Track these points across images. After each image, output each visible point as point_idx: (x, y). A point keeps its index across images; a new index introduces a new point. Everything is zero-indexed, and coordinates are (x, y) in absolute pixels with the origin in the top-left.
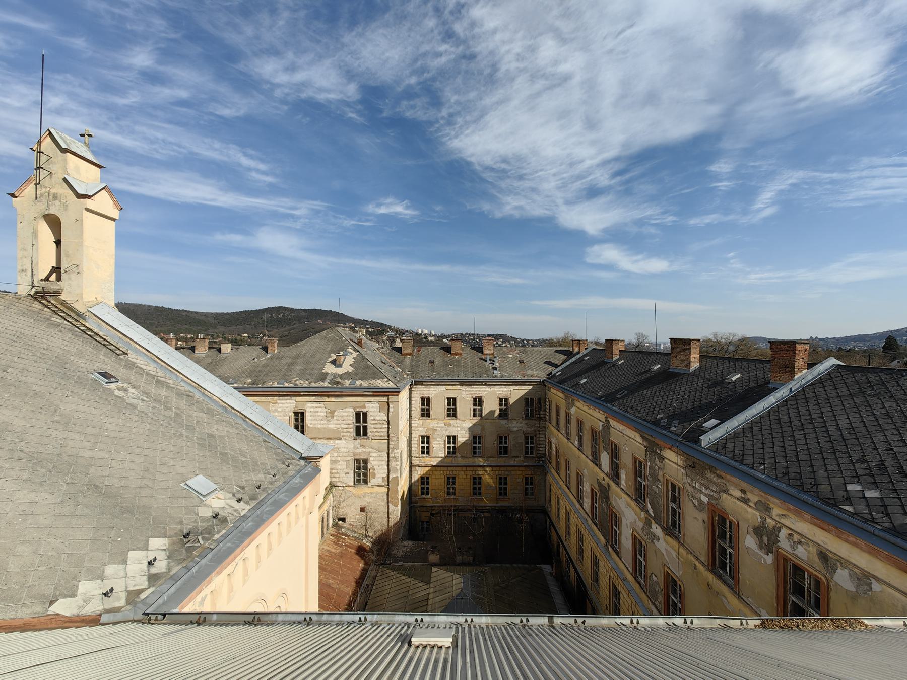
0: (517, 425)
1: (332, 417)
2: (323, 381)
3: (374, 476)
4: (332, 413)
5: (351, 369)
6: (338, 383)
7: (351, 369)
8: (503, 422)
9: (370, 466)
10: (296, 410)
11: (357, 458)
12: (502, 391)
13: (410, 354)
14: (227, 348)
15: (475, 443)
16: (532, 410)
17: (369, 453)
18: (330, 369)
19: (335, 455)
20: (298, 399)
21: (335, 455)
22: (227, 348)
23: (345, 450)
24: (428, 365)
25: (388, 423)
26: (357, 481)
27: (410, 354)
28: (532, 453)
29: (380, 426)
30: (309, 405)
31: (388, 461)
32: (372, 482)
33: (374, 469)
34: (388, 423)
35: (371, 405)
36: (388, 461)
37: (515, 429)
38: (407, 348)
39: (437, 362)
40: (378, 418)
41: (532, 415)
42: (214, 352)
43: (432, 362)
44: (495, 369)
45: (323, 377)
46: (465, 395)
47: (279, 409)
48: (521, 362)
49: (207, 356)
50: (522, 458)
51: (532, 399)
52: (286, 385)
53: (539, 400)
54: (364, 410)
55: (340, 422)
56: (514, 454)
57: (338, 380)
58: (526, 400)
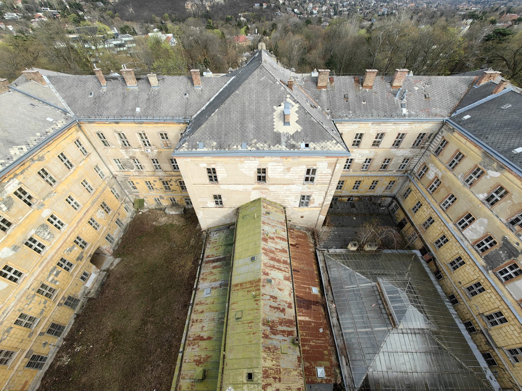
0: (404, 151)
1: (289, 172)
2: (279, 142)
3: (313, 203)
4: (288, 169)
5: (299, 128)
6: (293, 146)
7: (299, 128)
8: (394, 150)
9: (311, 198)
10: (259, 167)
11: (303, 195)
12: (403, 127)
13: (325, 87)
14: (153, 79)
15: (365, 162)
16: (420, 141)
17: (312, 192)
18: (279, 127)
19: (288, 193)
20: (261, 159)
21: (288, 193)
22: (153, 79)
23: (295, 190)
24: (343, 101)
25: (332, 175)
26: (301, 204)
27: (325, 87)
28: (403, 168)
29: (325, 177)
30: (270, 164)
31: (326, 196)
32: (311, 205)
33: (314, 199)
34: (332, 175)
35: (321, 164)
36: (326, 196)
37: (400, 155)
38: (322, 81)
39: (351, 97)
40: (324, 172)
41: (417, 145)
42: (143, 84)
43: (346, 97)
44: (402, 106)
45: (277, 138)
46: (370, 129)
47: (246, 167)
48: (371, 55)
49: (141, 90)
50: (394, 171)
51: (424, 134)
52: (249, 148)
53: (432, 134)
54: (315, 168)
55: (294, 175)
56: (390, 169)
57: (293, 142)
58: (421, 136)
